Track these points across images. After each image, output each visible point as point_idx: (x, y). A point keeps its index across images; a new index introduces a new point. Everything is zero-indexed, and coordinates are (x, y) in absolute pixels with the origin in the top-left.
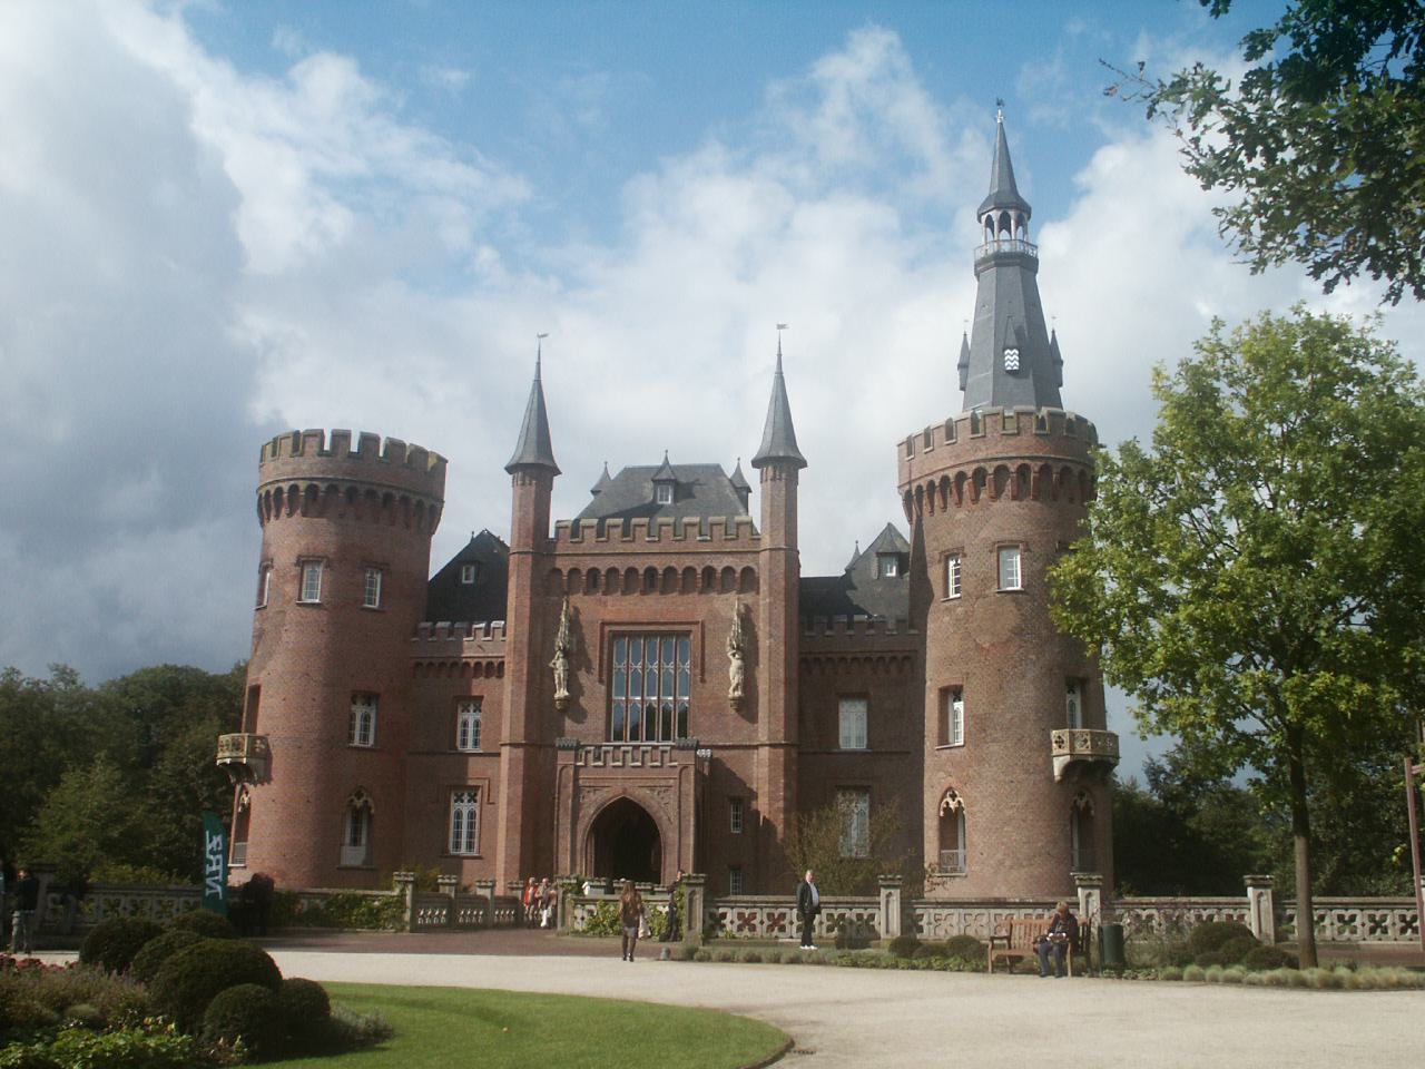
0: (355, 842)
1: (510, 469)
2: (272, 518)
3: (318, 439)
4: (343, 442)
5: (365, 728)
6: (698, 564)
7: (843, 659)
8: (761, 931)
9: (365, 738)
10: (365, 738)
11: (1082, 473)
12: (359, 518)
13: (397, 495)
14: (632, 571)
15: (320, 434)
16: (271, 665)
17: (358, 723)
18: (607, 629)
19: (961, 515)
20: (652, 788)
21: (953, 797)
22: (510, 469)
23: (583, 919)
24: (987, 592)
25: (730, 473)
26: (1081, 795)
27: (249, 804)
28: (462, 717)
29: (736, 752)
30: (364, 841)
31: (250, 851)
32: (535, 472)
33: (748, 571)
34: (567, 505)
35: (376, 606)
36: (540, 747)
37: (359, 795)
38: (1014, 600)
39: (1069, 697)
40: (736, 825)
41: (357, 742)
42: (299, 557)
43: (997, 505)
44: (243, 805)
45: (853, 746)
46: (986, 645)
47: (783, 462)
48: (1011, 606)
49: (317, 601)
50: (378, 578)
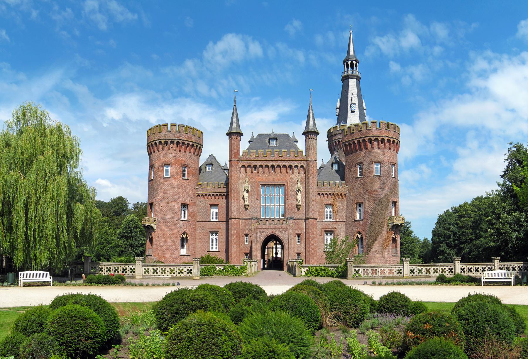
5: (184, 214)
9: (184, 217)
10: (184, 217)
15: (166, 125)
19: (363, 152)
21: (359, 234)
28: (212, 210)
35: (186, 178)
37: (184, 234)
40: (299, 242)
41: (182, 219)
43: (374, 150)
48: (378, 180)
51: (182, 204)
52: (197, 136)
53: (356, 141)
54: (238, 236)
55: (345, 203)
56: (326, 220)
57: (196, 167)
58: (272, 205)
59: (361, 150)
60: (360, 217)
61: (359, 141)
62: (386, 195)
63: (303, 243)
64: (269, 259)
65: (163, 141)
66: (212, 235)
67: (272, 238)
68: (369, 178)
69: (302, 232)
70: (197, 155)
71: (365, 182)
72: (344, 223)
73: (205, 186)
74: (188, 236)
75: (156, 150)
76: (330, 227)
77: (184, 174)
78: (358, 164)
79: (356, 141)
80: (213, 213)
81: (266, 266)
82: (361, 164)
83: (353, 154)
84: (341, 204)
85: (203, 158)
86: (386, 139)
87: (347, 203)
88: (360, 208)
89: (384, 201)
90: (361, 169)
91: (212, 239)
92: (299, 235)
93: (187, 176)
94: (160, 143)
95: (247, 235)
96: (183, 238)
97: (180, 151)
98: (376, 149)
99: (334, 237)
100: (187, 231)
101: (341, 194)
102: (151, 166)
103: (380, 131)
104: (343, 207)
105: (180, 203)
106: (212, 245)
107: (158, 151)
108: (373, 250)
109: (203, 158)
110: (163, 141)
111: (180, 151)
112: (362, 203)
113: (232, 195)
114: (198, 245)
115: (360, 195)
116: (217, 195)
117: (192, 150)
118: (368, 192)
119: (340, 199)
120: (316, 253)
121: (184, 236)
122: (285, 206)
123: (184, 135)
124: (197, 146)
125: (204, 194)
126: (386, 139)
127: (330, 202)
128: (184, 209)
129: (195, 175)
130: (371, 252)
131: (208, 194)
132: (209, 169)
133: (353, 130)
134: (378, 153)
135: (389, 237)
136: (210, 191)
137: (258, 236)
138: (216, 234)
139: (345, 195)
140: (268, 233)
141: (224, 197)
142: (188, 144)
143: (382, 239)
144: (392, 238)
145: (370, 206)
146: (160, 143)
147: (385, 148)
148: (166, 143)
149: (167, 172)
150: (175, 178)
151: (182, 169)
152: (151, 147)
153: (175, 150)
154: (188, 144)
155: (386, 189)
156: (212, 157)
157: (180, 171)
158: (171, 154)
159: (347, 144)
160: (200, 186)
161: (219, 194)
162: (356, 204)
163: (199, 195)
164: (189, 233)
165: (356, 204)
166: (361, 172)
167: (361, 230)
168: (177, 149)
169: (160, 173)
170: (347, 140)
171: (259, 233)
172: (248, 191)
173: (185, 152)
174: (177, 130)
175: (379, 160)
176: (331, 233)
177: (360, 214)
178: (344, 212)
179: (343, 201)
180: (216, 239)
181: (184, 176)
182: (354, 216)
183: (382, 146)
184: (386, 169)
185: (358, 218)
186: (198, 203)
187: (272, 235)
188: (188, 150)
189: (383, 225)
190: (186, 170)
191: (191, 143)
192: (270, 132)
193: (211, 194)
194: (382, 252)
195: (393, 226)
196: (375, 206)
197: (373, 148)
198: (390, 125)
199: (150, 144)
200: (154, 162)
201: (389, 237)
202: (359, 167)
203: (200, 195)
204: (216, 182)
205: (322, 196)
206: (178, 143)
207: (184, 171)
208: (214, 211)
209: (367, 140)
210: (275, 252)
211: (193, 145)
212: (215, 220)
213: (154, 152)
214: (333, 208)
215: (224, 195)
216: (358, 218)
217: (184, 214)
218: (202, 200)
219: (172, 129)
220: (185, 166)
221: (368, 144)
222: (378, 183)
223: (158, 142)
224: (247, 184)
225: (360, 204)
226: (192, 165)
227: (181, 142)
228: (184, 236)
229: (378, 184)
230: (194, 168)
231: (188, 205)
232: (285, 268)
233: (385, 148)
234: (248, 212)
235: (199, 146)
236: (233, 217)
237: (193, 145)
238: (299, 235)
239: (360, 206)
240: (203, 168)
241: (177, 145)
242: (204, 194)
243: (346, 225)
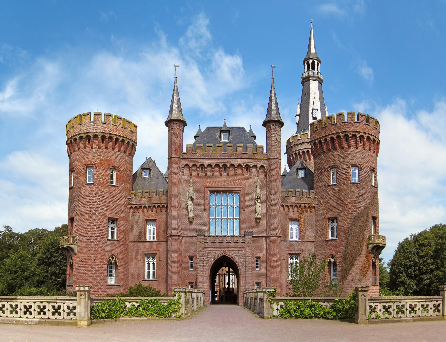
3: (89, 116)
8: (394, 314)
15: (89, 114)
23: (277, 309)
24: (347, 183)
25: (248, 130)
35: (115, 184)
40: (258, 267)
45: (294, 239)
46: (347, 202)
48: (356, 188)
49: (93, 182)
52: (128, 129)
53: (328, 138)
54: (180, 260)
55: (314, 218)
56: (290, 240)
57: (128, 170)
58: (224, 220)
59: (335, 149)
60: (333, 236)
61: (332, 138)
62: (365, 208)
63: (263, 268)
64: (220, 291)
65: (84, 136)
67: (224, 262)
68: (345, 186)
69: (262, 254)
70: (130, 155)
71: (340, 192)
72: (313, 244)
75: (76, 148)
76: (296, 249)
77: (112, 179)
78: (332, 168)
79: (328, 138)
80: (149, 230)
81: (216, 299)
82: (335, 167)
83: (325, 155)
84: (310, 219)
86: (366, 136)
87: (317, 218)
88: (333, 224)
89: (363, 216)
92: (258, 258)
93: (117, 182)
94: (81, 138)
95: (191, 258)
97: (106, 148)
98: (353, 149)
99: (300, 262)
101: (309, 207)
102: (72, 171)
103: (358, 125)
104: (312, 223)
105: (107, 217)
107: (79, 149)
108: (350, 278)
110: (84, 136)
111: (106, 148)
112: (336, 218)
114: (130, 271)
116: (154, 207)
117: (123, 148)
118: (344, 203)
119: (309, 213)
120: (280, 282)
122: (240, 219)
123: (111, 127)
124: (128, 142)
125: (138, 206)
126: (366, 136)
127: (295, 217)
129: (127, 180)
130: (347, 281)
131: (143, 206)
132: (145, 175)
133: (325, 124)
134: (355, 154)
135: (368, 262)
136: (145, 201)
137: (205, 257)
139: (314, 207)
141: (164, 210)
142: (117, 140)
143: (360, 264)
144: (371, 263)
145: (346, 221)
146: (81, 138)
147: (364, 148)
148: (88, 137)
149: (90, 176)
150: (100, 185)
151: (109, 173)
152: (70, 145)
154: (117, 140)
155: (365, 202)
156: (149, 160)
157: (107, 175)
158: (95, 153)
159: (317, 142)
160: (133, 195)
161: (156, 206)
162: (329, 219)
163: (131, 208)
165: (329, 219)
168: (103, 146)
170: (317, 137)
171: (206, 254)
173: (113, 149)
174: (103, 120)
175: (357, 163)
176: (297, 256)
177: (333, 232)
178: (313, 230)
179: (312, 216)
181: (112, 182)
182: (326, 235)
183: (360, 145)
185: (330, 238)
186: (130, 218)
188: (117, 147)
189: (361, 246)
190: (115, 174)
191: (120, 139)
192: (222, 125)
193: (147, 206)
194: (360, 280)
195: (374, 247)
196: (352, 222)
197: (349, 147)
198: (370, 119)
199: (69, 142)
200: (74, 164)
201: (368, 262)
202: (332, 171)
203: (134, 206)
204: (153, 191)
205: (286, 208)
206: (103, 138)
207: (112, 175)
208: (151, 229)
209: (342, 136)
210: (227, 281)
211: (123, 141)
212: (152, 239)
213: (74, 151)
214: (300, 226)
215: (163, 206)
216: (330, 238)
218: (136, 213)
219: (95, 119)
221: (344, 142)
223: (77, 137)
224: (191, 190)
225: (332, 220)
226: (122, 169)
227: (107, 136)
229: (357, 194)
230: (126, 171)
231: (117, 219)
232: (241, 301)
235: (131, 143)
236: (173, 234)
237: (123, 141)
238: (258, 258)
239: (333, 222)
240: (139, 174)
241: (103, 141)
242: (138, 206)
243: (315, 246)
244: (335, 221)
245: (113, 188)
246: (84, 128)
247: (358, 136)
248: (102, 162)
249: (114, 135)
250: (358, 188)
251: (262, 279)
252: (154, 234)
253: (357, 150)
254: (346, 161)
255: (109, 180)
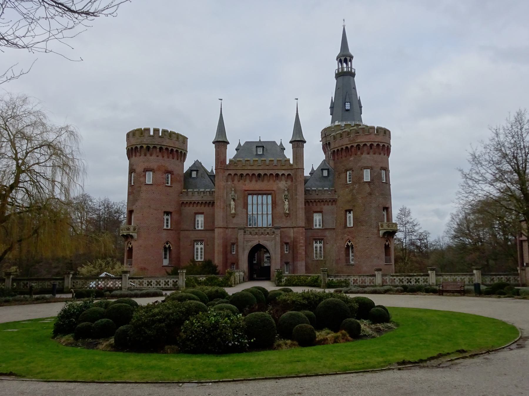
0: (165, 258)
1: (214, 143)
2: (134, 157)
4: (157, 132)
5: (167, 223)
6: (274, 173)
7: (315, 201)
9: (167, 226)
10: (167, 226)
11: (388, 146)
12: (163, 157)
13: (175, 149)
14: (253, 174)
15: (148, 130)
16: (137, 204)
17: (165, 221)
18: (246, 192)
19: (352, 159)
20: (267, 241)
21: (350, 242)
22: (214, 143)
26: (387, 241)
27: (132, 247)
29: (285, 229)
30: (168, 257)
31: (133, 262)
32: (221, 143)
33: (289, 175)
34: (231, 153)
35: (169, 185)
36: (227, 228)
37: (167, 244)
38: (369, 184)
39: (384, 213)
41: (165, 227)
42: (144, 169)
43: (363, 156)
44: (129, 247)
47: (298, 143)
48: (367, 186)
49: (151, 183)
50: (170, 176)
51: (165, 212)
63: (291, 252)
65: (145, 146)
66: (197, 244)
73: (190, 194)
74: (171, 246)
77: (168, 181)
78: (346, 171)
85: (187, 165)
88: (350, 215)
90: (350, 176)
91: (197, 249)
96: (165, 248)
98: (365, 156)
100: (170, 240)
103: (368, 137)
106: (197, 255)
109: (187, 165)
110: (145, 146)
113: (218, 204)
115: (349, 202)
121: (167, 246)
124: (181, 152)
128: (167, 217)
134: (367, 158)
138: (201, 244)
140: (255, 243)
153: (158, 156)
158: (154, 160)
164: (172, 243)
166: (350, 178)
167: (350, 238)
169: (142, 179)
172: (234, 200)
174: (160, 135)
180: (201, 249)
181: (168, 183)
184: (375, 174)
187: (259, 244)
212: (200, 228)
217: (167, 223)
220: (168, 172)
222: (367, 189)
225: (350, 211)
228: (167, 246)
231: (171, 213)
233: (374, 154)
234: (235, 221)
244: (352, 212)
245: (169, 188)
246: (145, 140)
247: (368, 145)
248: (159, 169)
249: (169, 146)
250: (370, 186)
251: (290, 260)
252: (202, 224)
253: (368, 156)
254: (359, 164)
255: (165, 181)
